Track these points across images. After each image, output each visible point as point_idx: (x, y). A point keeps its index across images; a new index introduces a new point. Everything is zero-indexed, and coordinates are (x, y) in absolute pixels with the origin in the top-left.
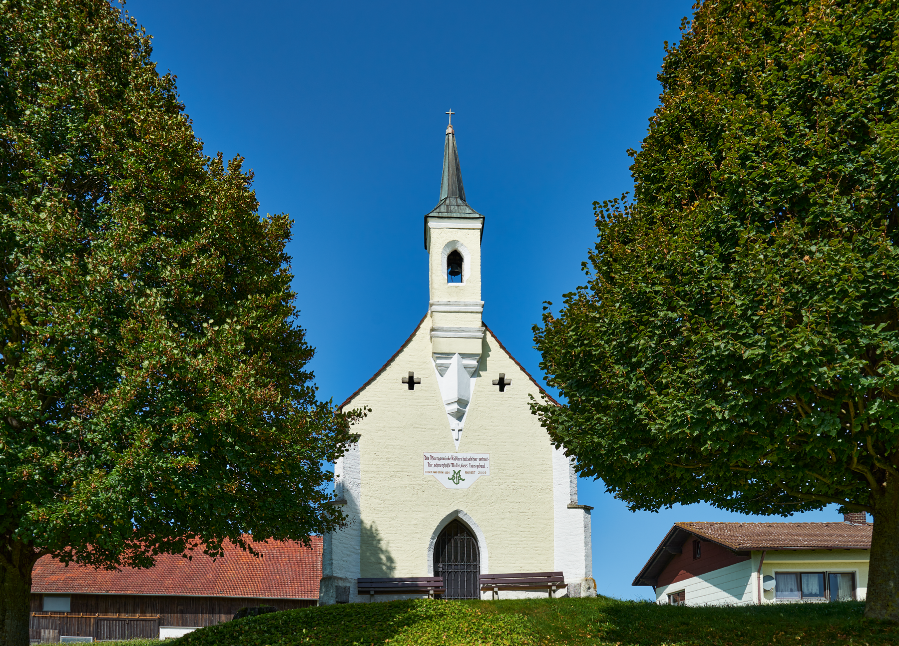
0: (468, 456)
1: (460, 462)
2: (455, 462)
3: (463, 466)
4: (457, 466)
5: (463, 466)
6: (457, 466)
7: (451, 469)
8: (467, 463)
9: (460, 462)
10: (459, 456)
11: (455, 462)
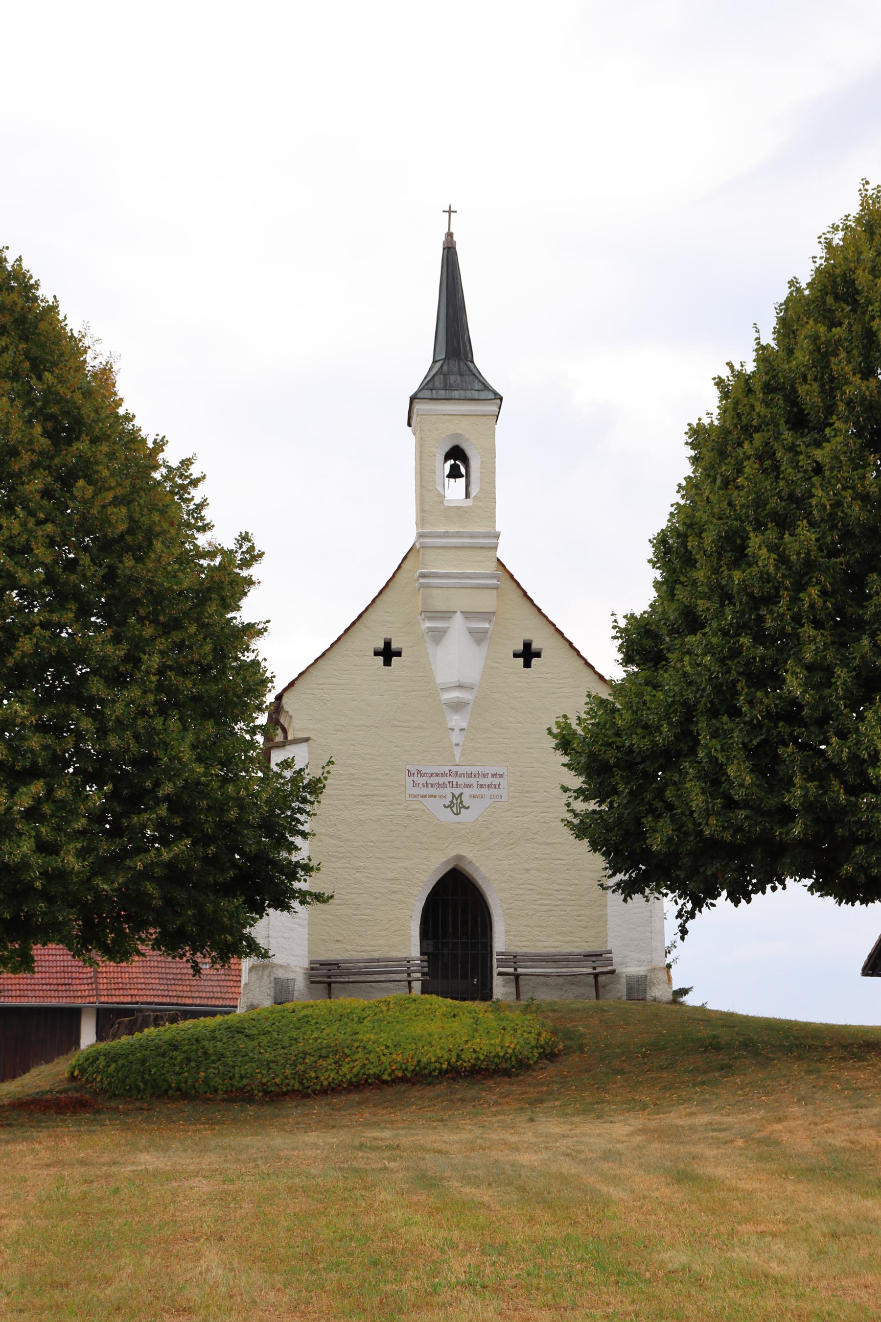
0: (475, 770)
1: (462, 780)
2: (454, 780)
3: (466, 786)
4: (458, 785)
5: (466, 786)
6: (458, 785)
7: (448, 791)
8: (472, 781)
9: (462, 780)
10: (461, 770)
11: (454, 780)
